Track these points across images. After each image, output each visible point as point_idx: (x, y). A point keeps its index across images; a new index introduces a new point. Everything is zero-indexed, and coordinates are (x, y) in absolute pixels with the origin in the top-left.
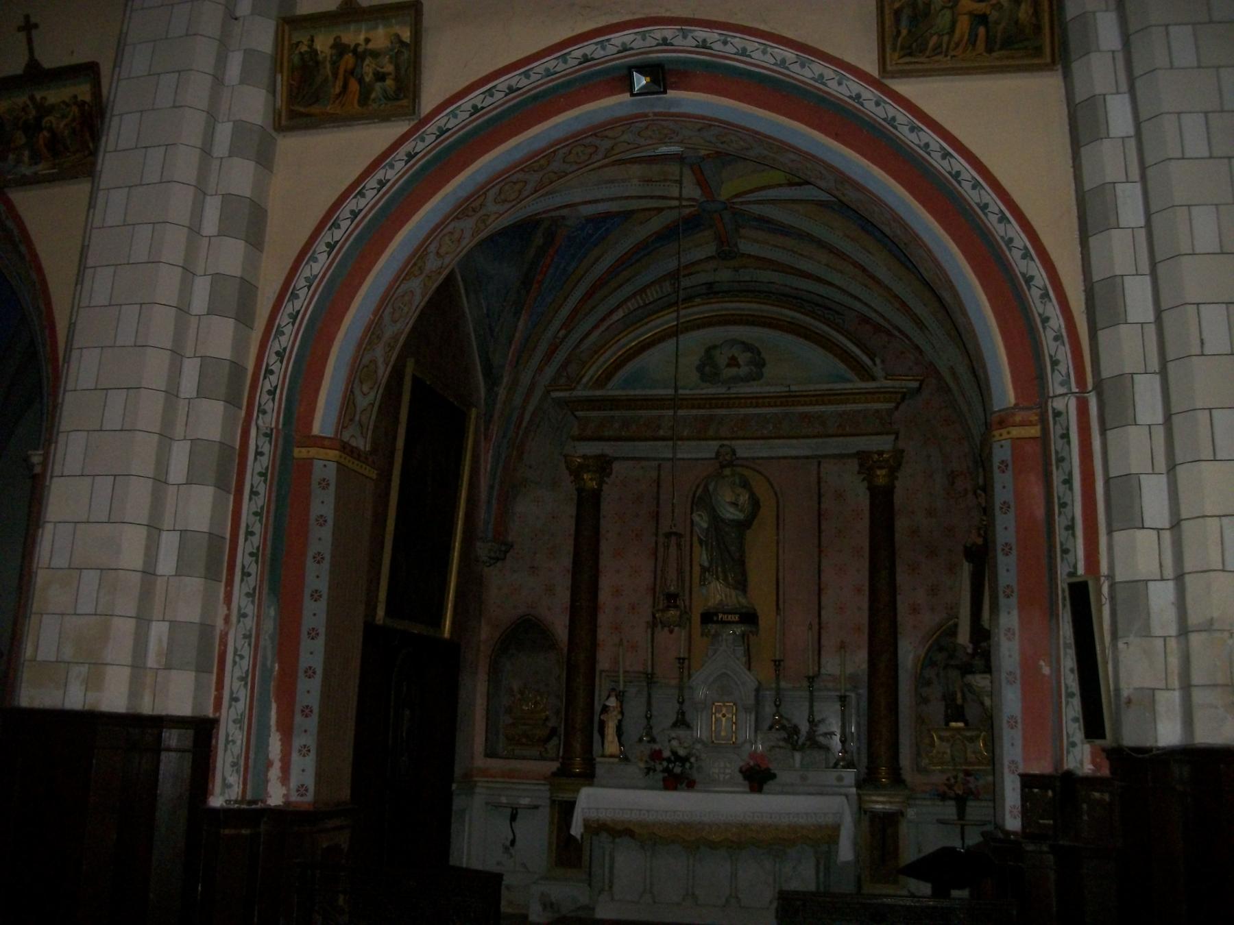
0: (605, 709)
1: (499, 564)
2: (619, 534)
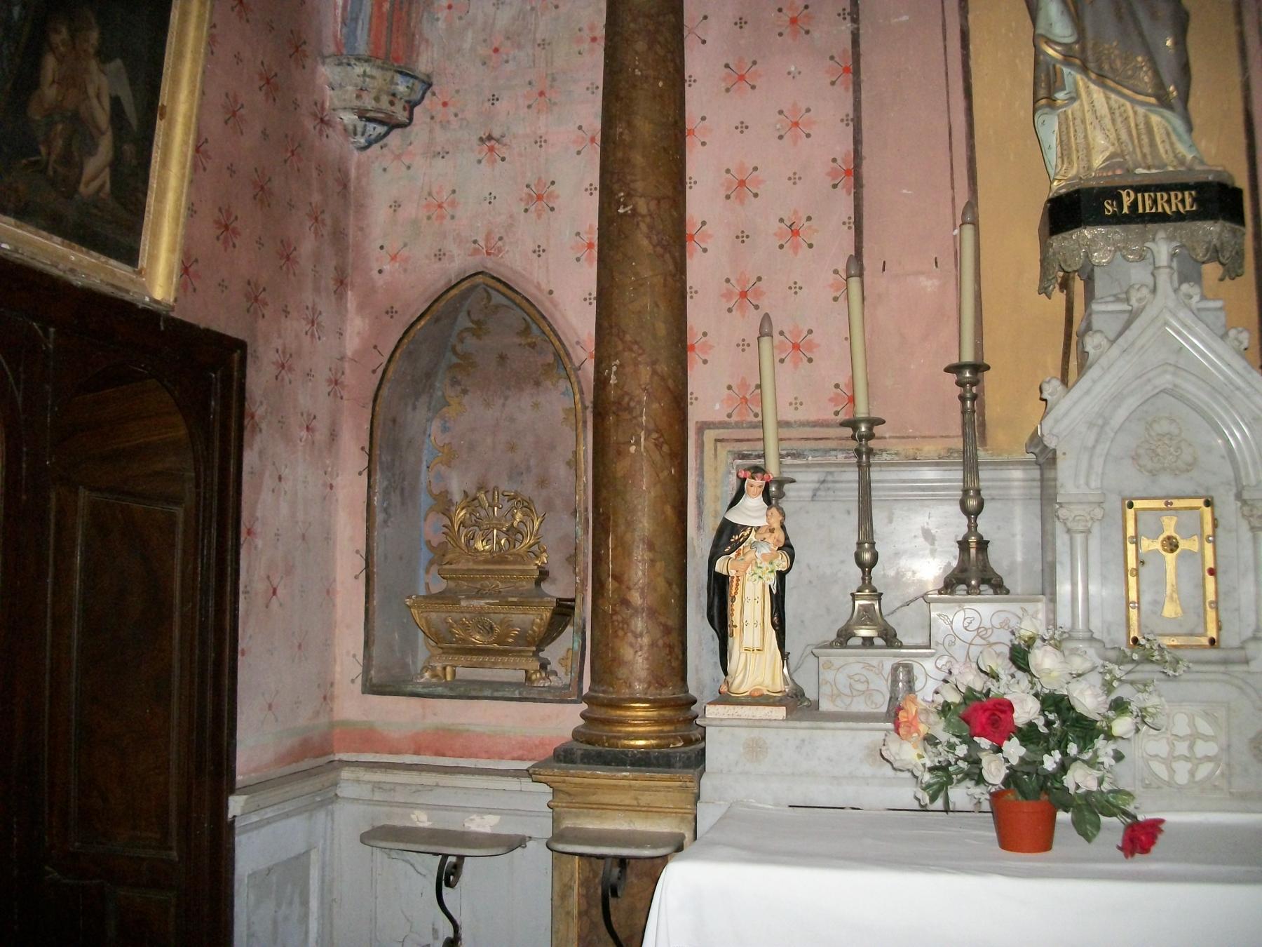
1: (395, 138)
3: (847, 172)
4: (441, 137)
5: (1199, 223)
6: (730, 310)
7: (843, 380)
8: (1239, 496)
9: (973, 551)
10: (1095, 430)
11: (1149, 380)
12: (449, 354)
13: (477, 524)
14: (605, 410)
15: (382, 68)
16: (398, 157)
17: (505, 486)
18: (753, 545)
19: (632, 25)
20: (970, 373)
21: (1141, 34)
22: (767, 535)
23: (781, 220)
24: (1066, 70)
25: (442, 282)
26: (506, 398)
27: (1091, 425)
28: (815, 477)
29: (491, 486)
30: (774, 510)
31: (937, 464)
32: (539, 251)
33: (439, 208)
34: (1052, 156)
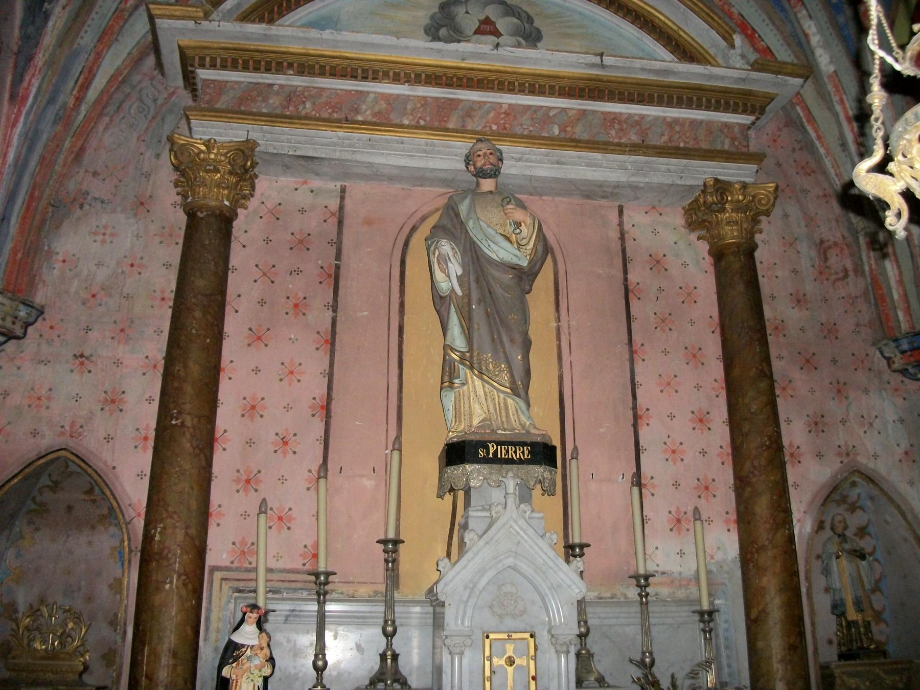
0: (231, 652)
1: (11, 346)
2: (262, 303)
3: (322, 407)
4: (46, 350)
5: (531, 466)
6: (238, 491)
7: (309, 543)
8: (549, 631)
9: (389, 661)
10: (468, 591)
11: (501, 561)
12: (29, 502)
13: (38, 629)
14: (149, 557)
15: (11, 299)
16: (12, 359)
17: (60, 600)
18: (249, 658)
19: (193, 300)
20: (391, 545)
21: (505, 352)
22: (258, 652)
23: (277, 434)
24: (461, 367)
25: (35, 453)
26: (68, 537)
27: (466, 587)
28: (288, 607)
29: (50, 600)
30: (264, 634)
31: (368, 601)
32: (108, 439)
33: (37, 400)
34: (450, 415)
